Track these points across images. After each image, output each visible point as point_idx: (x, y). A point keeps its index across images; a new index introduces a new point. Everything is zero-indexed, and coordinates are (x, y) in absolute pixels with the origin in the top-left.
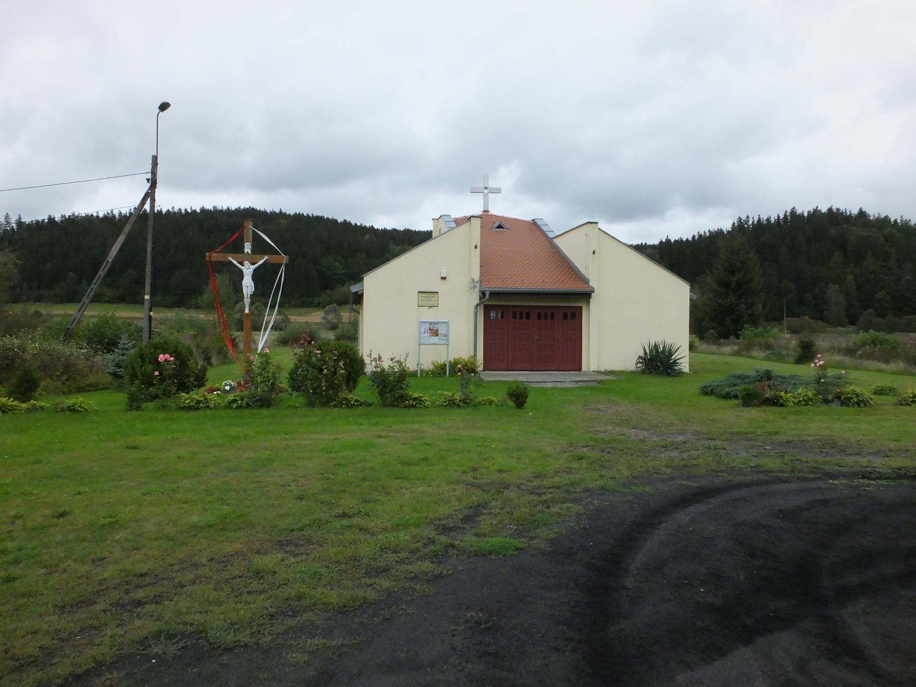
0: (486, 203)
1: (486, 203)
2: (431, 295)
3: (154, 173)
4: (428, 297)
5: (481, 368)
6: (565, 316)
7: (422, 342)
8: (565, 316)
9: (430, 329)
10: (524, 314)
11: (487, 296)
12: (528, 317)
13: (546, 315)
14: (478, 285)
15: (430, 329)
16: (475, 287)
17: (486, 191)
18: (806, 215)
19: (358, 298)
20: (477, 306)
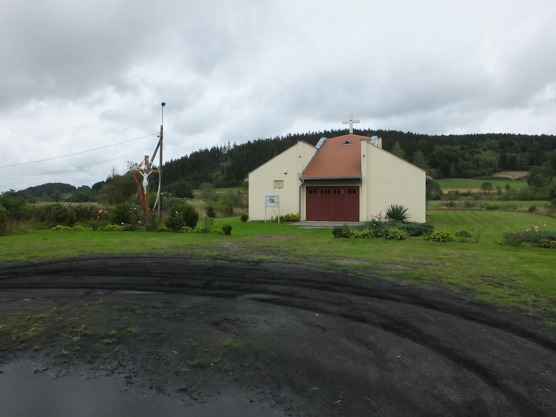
3: (162, 133)
4: (279, 183)
5: (305, 219)
6: (350, 192)
8: (350, 192)
10: (326, 191)
12: (329, 193)
17: (351, 122)
18: (209, 150)
19: (247, 185)
20: (300, 187)
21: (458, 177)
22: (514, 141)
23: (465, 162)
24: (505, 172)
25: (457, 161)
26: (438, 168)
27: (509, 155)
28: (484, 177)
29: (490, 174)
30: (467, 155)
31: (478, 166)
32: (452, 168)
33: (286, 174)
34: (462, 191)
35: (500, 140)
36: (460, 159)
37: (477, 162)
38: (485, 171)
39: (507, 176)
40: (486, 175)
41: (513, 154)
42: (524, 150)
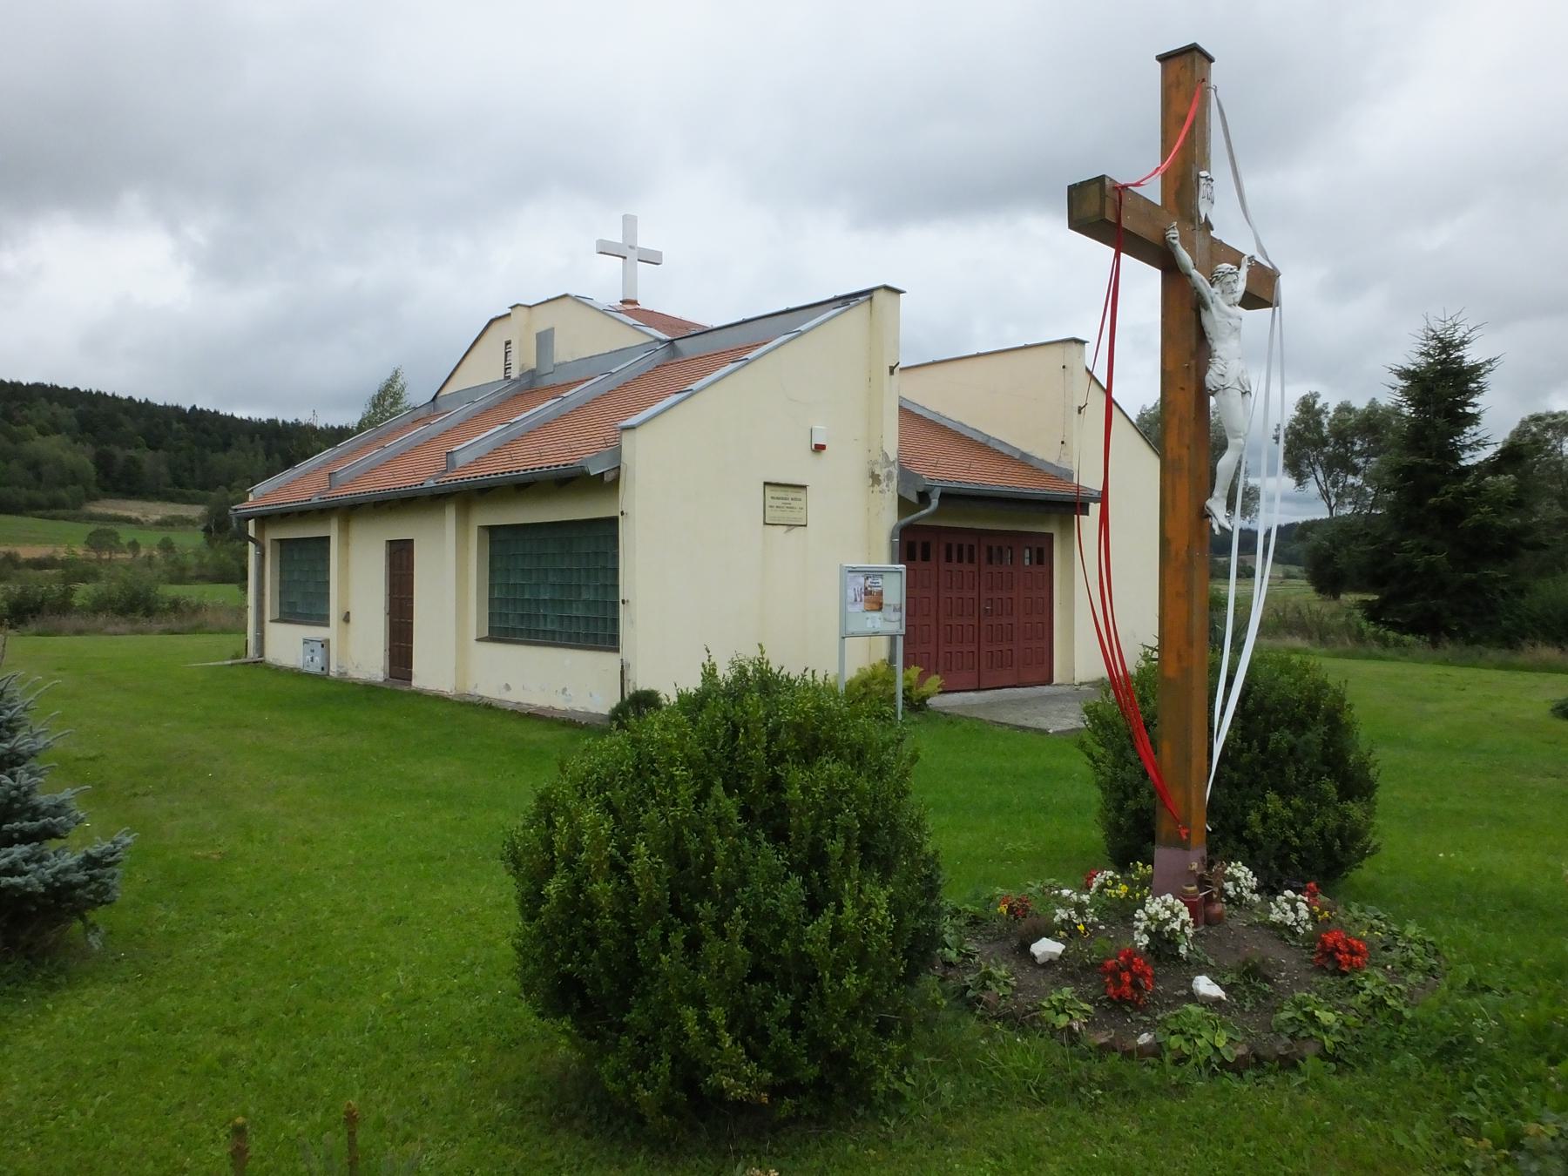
0: (629, 279)
2: (791, 494)
7: (851, 629)
9: (867, 593)
11: (935, 502)
13: (926, 549)
14: (896, 472)
16: (889, 476)
22: (121, 416)
24: (109, 502)
27: (120, 454)
28: (62, 512)
29: (77, 505)
31: (39, 477)
33: (819, 448)
35: (80, 407)
37: (34, 466)
38: (62, 494)
39: (126, 514)
40: (64, 506)
41: (132, 453)
42: (154, 446)
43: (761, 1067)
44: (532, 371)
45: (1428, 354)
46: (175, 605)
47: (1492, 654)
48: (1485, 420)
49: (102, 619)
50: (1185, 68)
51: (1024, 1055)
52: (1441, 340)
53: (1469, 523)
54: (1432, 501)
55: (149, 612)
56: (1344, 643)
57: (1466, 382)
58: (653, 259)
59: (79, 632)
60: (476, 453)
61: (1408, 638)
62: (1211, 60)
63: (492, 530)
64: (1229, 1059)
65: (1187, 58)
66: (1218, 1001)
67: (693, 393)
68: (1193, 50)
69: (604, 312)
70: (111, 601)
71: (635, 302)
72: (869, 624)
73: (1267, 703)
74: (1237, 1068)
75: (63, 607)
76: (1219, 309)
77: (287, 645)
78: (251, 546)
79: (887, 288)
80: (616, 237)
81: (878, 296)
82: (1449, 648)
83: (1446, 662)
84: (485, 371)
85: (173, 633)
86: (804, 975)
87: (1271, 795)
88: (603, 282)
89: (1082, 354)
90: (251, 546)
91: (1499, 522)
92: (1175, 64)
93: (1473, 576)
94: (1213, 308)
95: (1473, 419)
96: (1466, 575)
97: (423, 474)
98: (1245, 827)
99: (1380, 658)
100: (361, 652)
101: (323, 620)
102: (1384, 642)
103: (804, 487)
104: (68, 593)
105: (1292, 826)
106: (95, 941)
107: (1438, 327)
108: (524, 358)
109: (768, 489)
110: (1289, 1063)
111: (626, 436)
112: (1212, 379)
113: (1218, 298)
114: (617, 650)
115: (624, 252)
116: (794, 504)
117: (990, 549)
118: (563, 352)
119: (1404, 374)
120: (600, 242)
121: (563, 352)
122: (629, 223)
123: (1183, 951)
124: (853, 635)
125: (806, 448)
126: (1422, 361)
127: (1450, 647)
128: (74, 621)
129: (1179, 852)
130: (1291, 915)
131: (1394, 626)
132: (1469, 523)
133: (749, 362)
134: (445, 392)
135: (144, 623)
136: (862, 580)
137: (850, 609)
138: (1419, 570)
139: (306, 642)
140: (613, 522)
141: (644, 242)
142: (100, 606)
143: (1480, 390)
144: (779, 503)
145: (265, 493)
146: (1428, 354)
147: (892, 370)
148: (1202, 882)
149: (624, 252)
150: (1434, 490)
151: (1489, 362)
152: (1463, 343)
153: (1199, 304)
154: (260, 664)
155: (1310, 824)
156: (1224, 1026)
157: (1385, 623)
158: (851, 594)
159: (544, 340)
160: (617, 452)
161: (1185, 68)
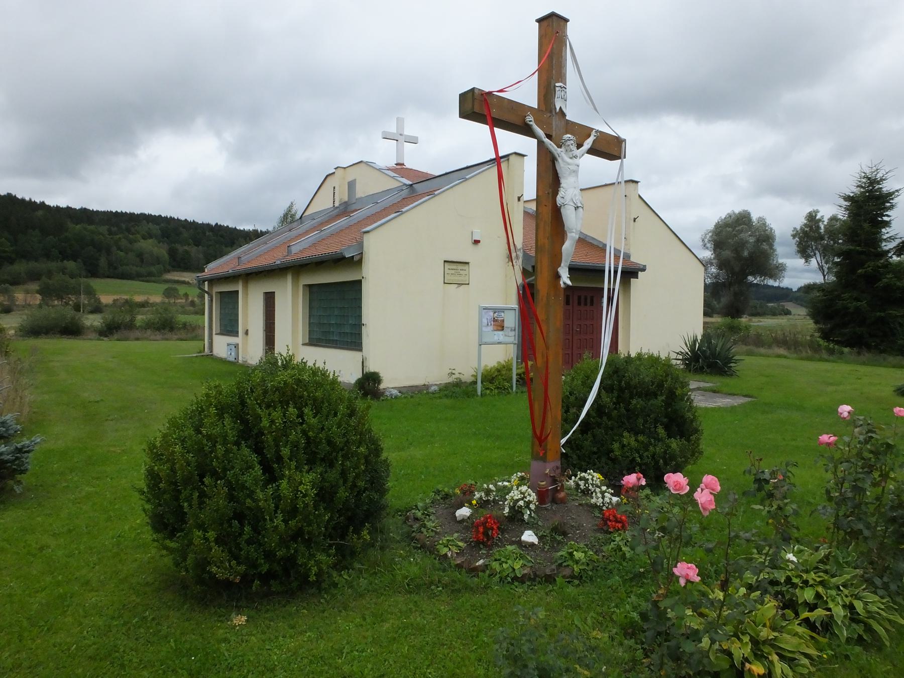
0: (400, 152)
1: (400, 152)
2: (460, 267)
7: (484, 340)
9: (495, 320)
15: (495, 320)
21: (108, 277)
22: (181, 229)
23: (122, 254)
24: (175, 273)
25: (108, 252)
26: (79, 260)
27: (181, 248)
28: (153, 278)
29: (160, 274)
30: (124, 243)
31: (142, 261)
32: (103, 262)
33: (477, 242)
34: (139, 299)
36: (114, 248)
37: (140, 255)
38: (153, 269)
39: (183, 279)
40: (154, 276)
41: (186, 248)
42: (197, 243)
43: (239, 564)
44: (345, 202)
45: (861, 187)
46: (185, 326)
47: (891, 359)
48: (893, 224)
49: (149, 332)
50: (552, 27)
51: (413, 565)
52: (869, 179)
53: (880, 284)
54: (860, 271)
55: (172, 329)
56: (807, 352)
57: (884, 203)
58: (413, 141)
59: (137, 339)
60: (302, 247)
61: (846, 350)
62: (566, 20)
63: (310, 286)
64: (519, 576)
65: (550, 19)
66: (532, 544)
67: (403, 213)
68: (553, 16)
69: (379, 170)
70: (153, 323)
71: (403, 164)
72: (496, 339)
73: (632, 383)
74: (522, 580)
75: (130, 326)
76: (563, 160)
77: (221, 346)
78: (206, 295)
79: (516, 153)
80: (393, 129)
81: (512, 158)
82: (867, 356)
83: (864, 364)
84: (324, 203)
85: (182, 340)
86: (256, 519)
87: (626, 434)
88: (384, 155)
89: (636, 189)
90: (206, 295)
91: (898, 283)
92: (545, 23)
93: (883, 314)
94: (560, 160)
95: (887, 224)
96: (878, 314)
97: (277, 258)
98: (612, 451)
99: (827, 361)
100: (252, 351)
101: (235, 333)
102: (831, 352)
103: (467, 263)
104: (133, 320)
105: (638, 451)
106: (18, 489)
107: (868, 171)
108: (343, 195)
109: (447, 266)
110: (550, 579)
111: (366, 237)
112: (559, 200)
113: (563, 154)
114: (361, 350)
115: (398, 138)
116: (462, 272)
117: (579, 298)
118: (360, 193)
119: (847, 198)
120: (384, 132)
121: (360, 193)
122: (400, 122)
123: (526, 517)
124: (486, 344)
125: (470, 242)
126: (858, 191)
127: (867, 355)
128: (138, 334)
129: (540, 463)
130: (601, 500)
131: (837, 343)
132: (880, 284)
133: (436, 195)
134: (306, 214)
135: (169, 335)
136: (492, 314)
137: (484, 329)
138: (851, 310)
139: (228, 345)
140: (359, 283)
141: (407, 132)
142: (149, 326)
143: (892, 207)
144: (453, 272)
145: (214, 268)
146: (861, 187)
147: (519, 199)
148: (554, 481)
149: (398, 138)
150: (862, 265)
151: (897, 191)
152: (882, 180)
153: (553, 159)
154: (211, 356)
155: (647, 450)
156: (522, 557)
157: (833, 341)
158: (485, 321)
159: (352, 185)
160: (361, 245)
161: (552, 27)
